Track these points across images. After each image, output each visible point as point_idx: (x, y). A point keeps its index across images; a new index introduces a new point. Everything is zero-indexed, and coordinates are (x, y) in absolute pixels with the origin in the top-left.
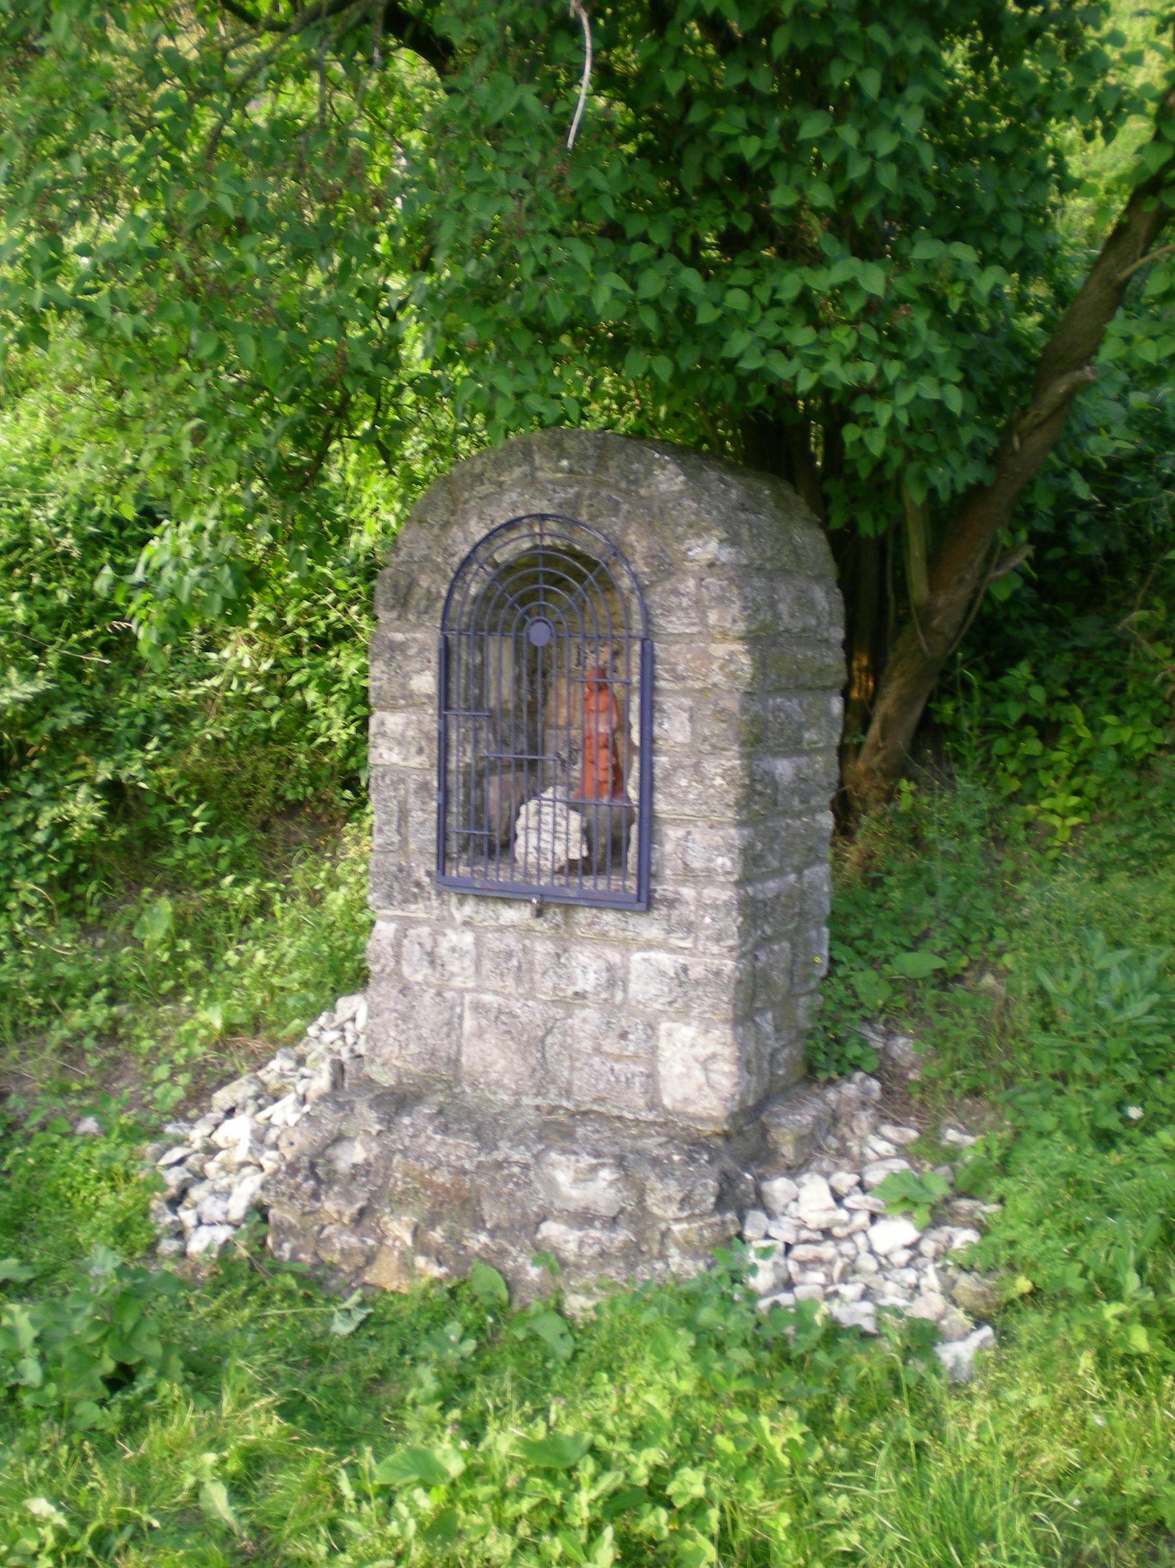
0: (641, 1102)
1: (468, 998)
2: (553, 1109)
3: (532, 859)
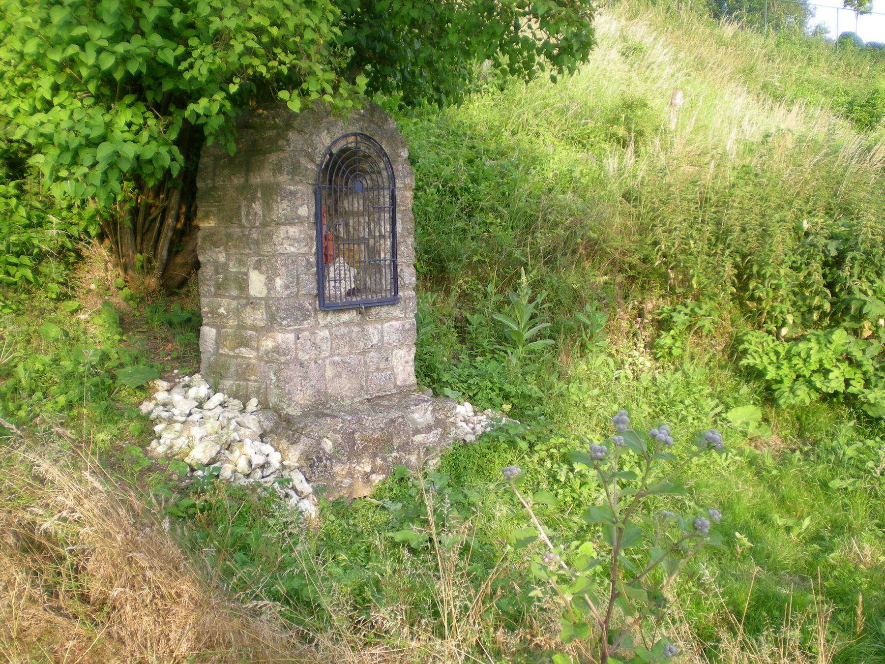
1: (328, 361)
3: (332, 292)
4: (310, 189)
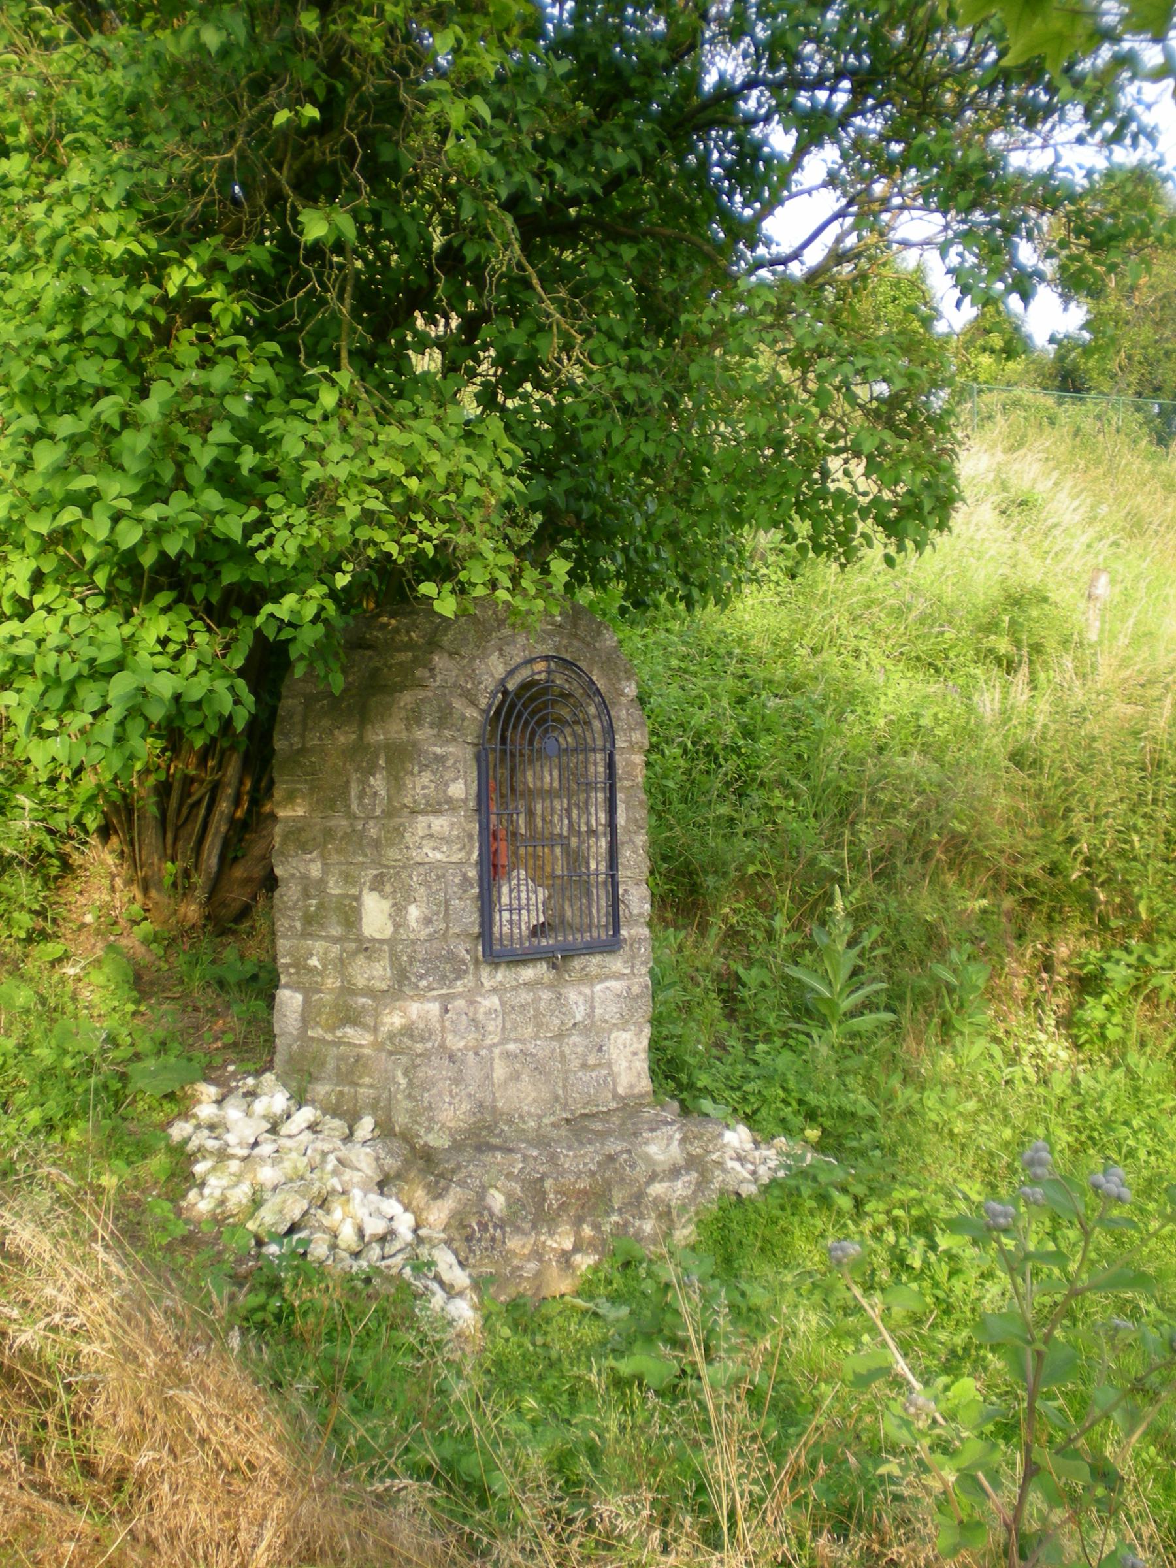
1: (497, 1051)
3: (506, 930)
4: (470, 752)
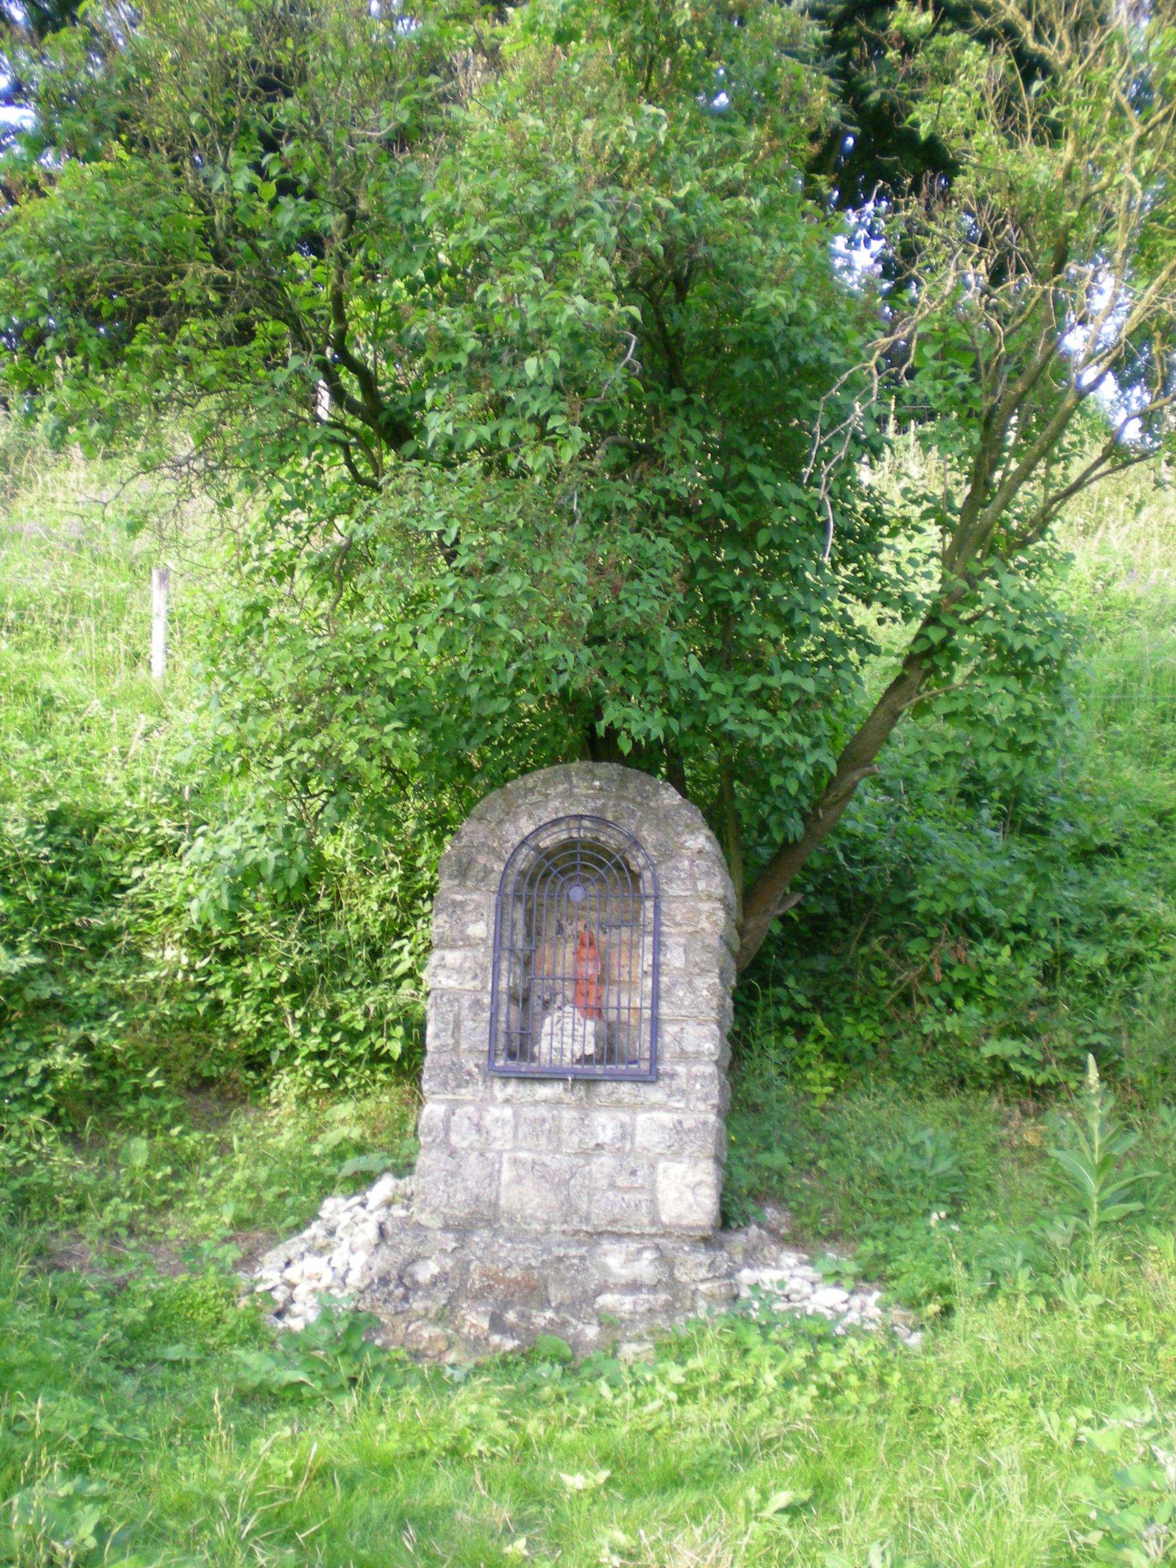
0: (646, 1221)
1: (506, 1156)
2: (577, 1232)
4: (494, 897)
